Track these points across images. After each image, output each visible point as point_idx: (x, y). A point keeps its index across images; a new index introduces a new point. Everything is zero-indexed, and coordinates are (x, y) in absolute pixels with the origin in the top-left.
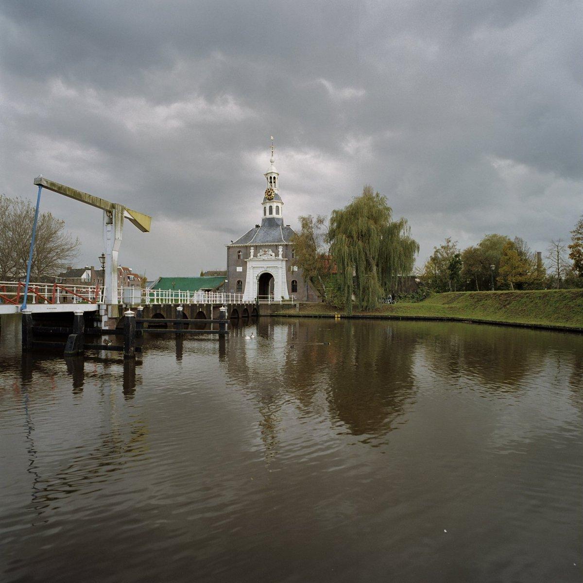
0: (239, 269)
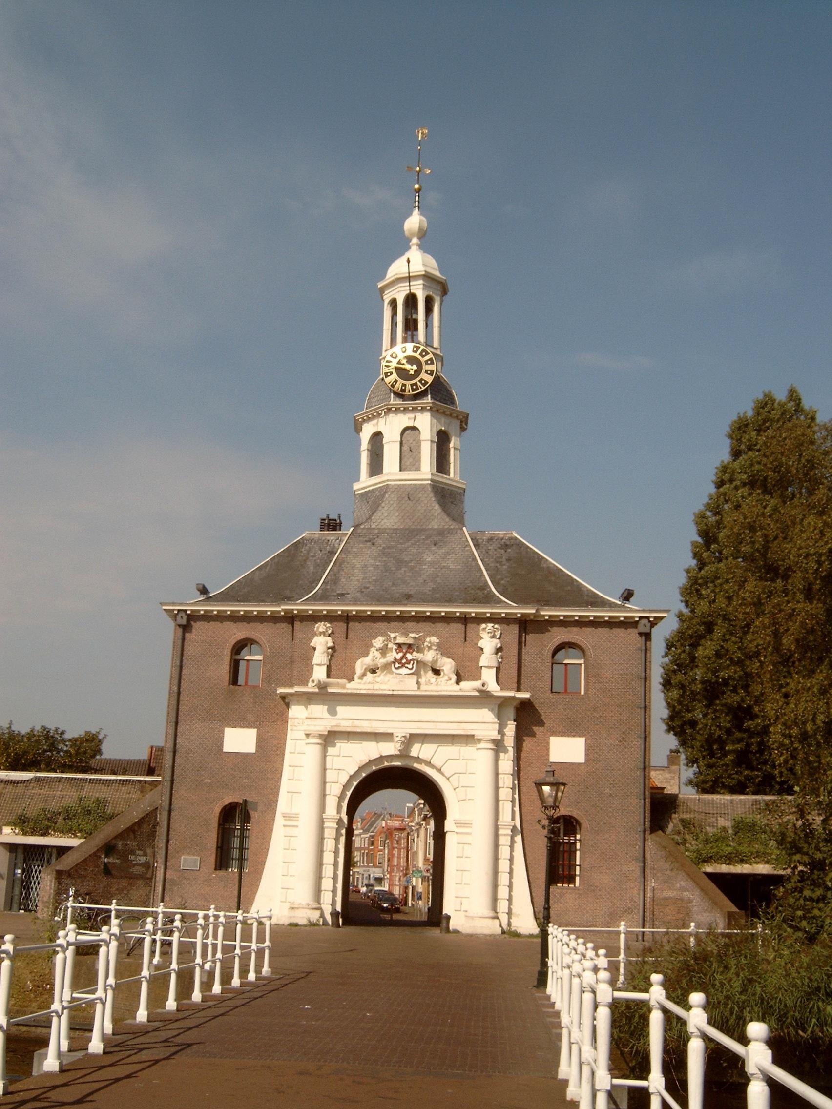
0: (240, 740)
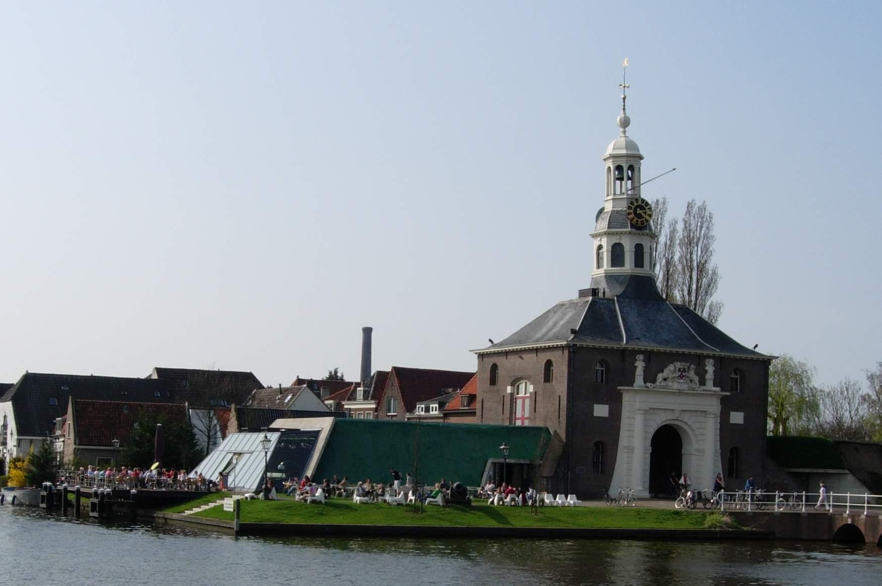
0: (601, 410)
